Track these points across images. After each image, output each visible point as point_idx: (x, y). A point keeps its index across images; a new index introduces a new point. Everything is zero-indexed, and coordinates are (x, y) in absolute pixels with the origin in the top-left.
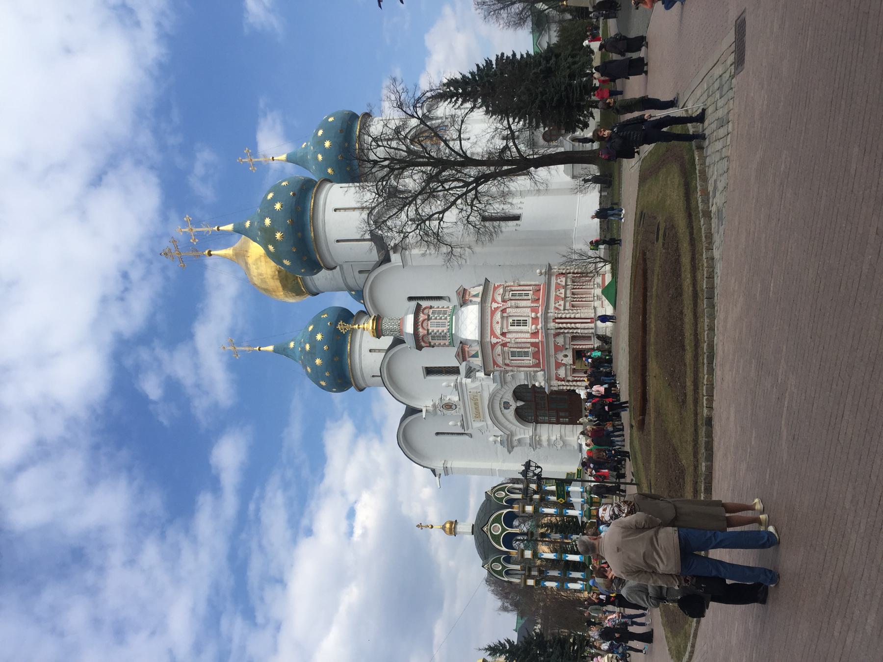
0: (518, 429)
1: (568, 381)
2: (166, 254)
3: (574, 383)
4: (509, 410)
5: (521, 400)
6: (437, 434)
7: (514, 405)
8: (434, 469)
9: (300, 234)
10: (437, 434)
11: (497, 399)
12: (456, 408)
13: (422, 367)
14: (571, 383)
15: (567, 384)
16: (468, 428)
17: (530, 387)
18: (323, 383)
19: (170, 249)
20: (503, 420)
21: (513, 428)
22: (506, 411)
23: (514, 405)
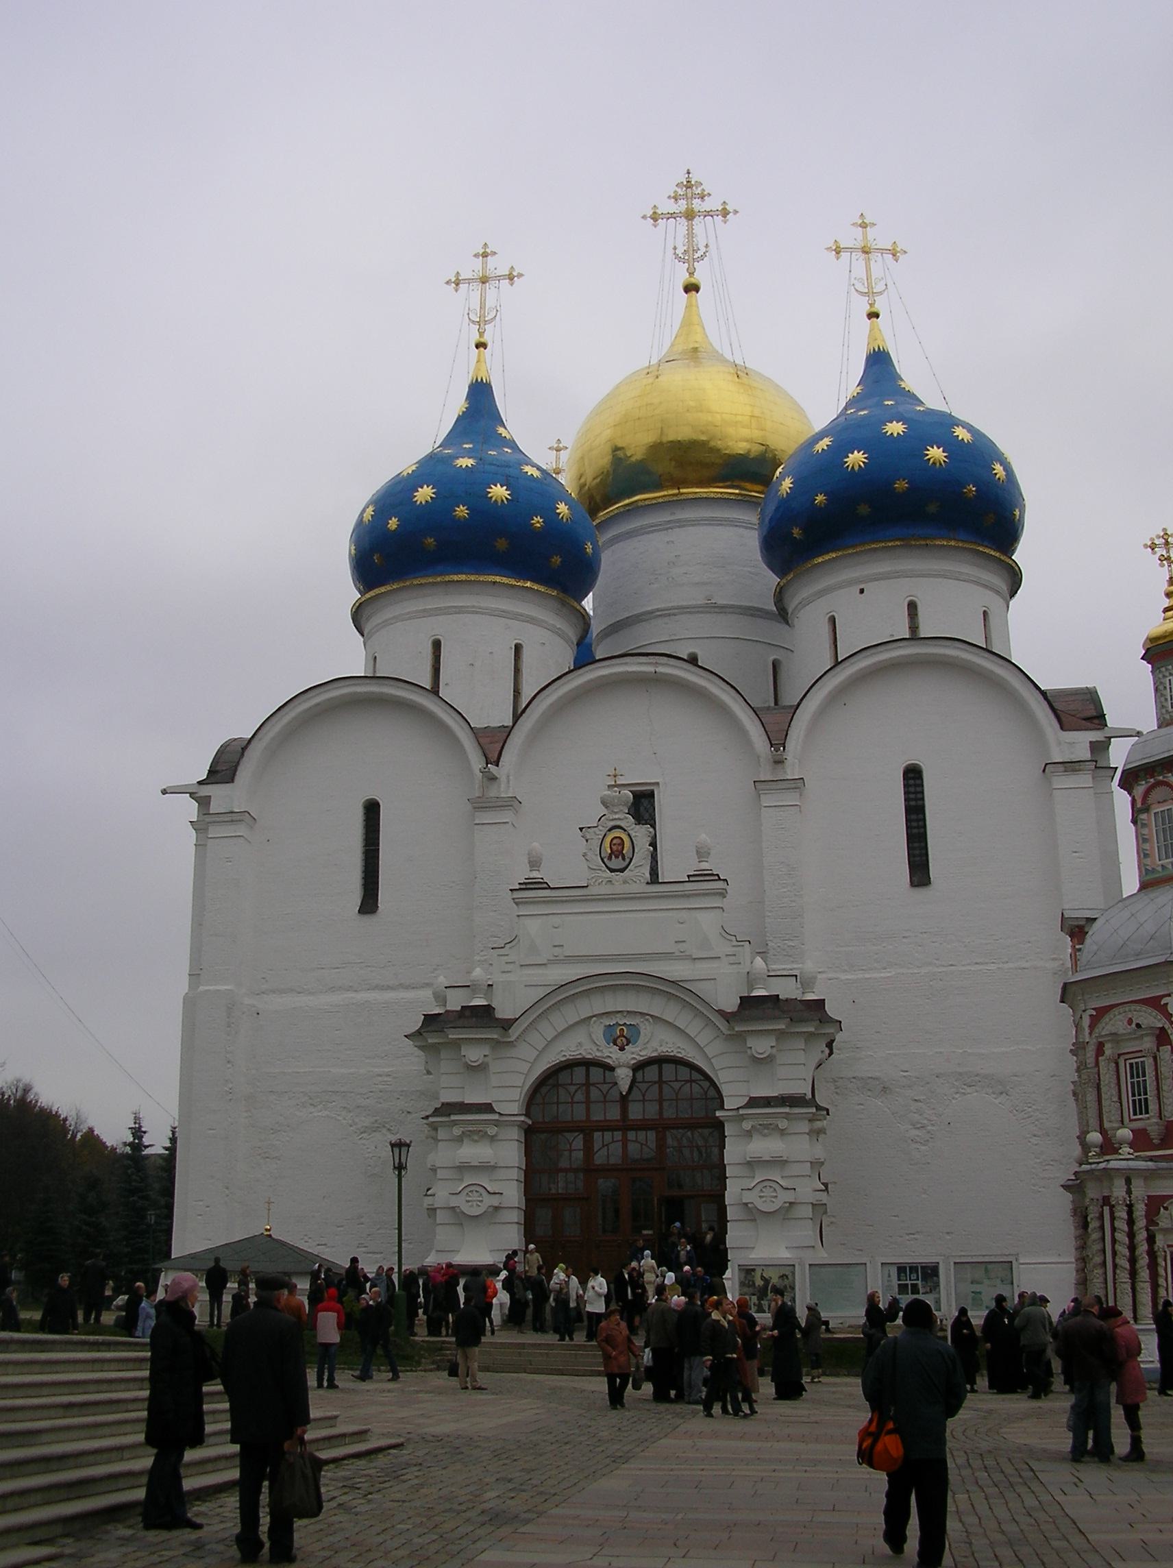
0: (525, 1067)
1: (1151, 1239)
2: (689, 185)
3: (1144, 1261)
4: (601, 1041)
5: (633, 1082)
6: (372, 810)
7: (623, 1059)
8: (232, 780)
9: (932, 508)
10: (372, 810)
11: (655, 1006)
12: (612, 871)
13: (657, 784)
14: (1143, 1248)
15: (1142, 1236)
16: (517, 904)
17: (718, 1114)
18: (425, 494)
19: (702, 197)
20: (571, 1014)
21: (525, 1052)
22: (598, 1030)
23: (623, 1059)
